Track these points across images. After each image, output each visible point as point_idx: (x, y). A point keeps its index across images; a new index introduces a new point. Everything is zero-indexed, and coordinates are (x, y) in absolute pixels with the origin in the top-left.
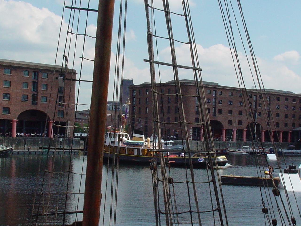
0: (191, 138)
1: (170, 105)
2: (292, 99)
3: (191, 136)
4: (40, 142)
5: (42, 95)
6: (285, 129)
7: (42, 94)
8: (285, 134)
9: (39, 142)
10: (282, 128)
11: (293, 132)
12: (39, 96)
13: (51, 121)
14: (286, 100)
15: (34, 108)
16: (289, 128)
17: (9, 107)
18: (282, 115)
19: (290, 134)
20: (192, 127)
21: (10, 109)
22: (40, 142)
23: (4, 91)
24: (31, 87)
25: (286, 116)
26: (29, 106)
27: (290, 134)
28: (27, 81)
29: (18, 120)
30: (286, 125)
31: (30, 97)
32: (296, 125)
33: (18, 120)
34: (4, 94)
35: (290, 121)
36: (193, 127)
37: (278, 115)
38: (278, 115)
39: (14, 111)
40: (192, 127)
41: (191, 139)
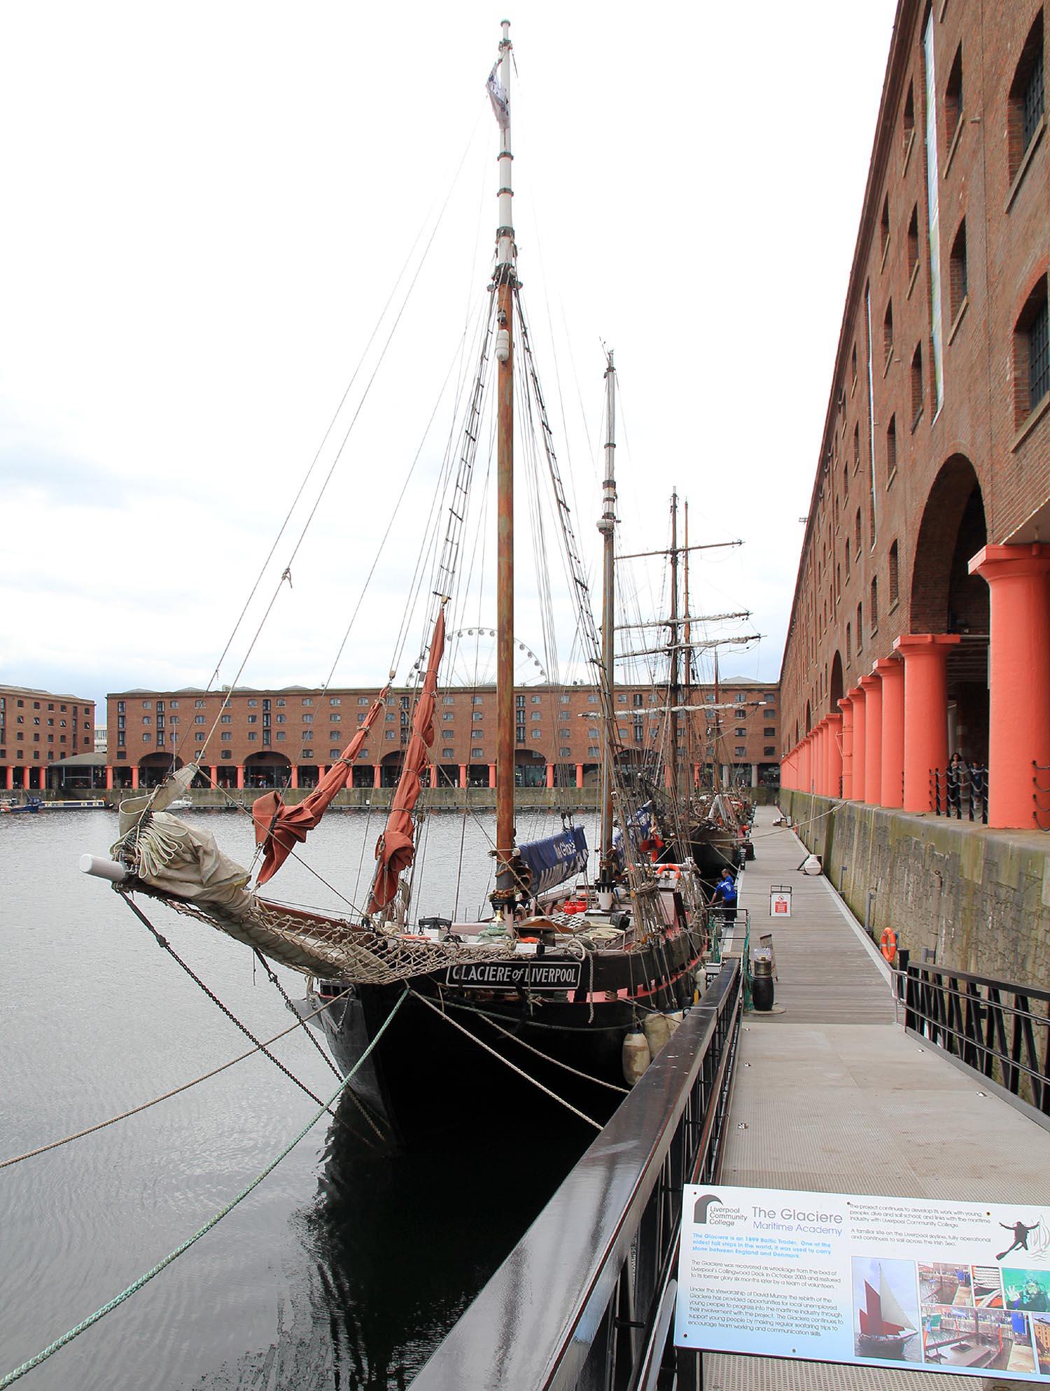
2: (47, 704)
6: (36, 764)
8: (35, 772)
10: (28, 762)
11: (50, 770)
14: (37, 706)
16: (44, 762)
18: (29, 737)
19: (43, 774)
25: (37, 737)
27: (43, 774)
30: (37, 755)
32: (57, 755)
35: (44, 747)
37: (20, 736)
38: (20, 736)
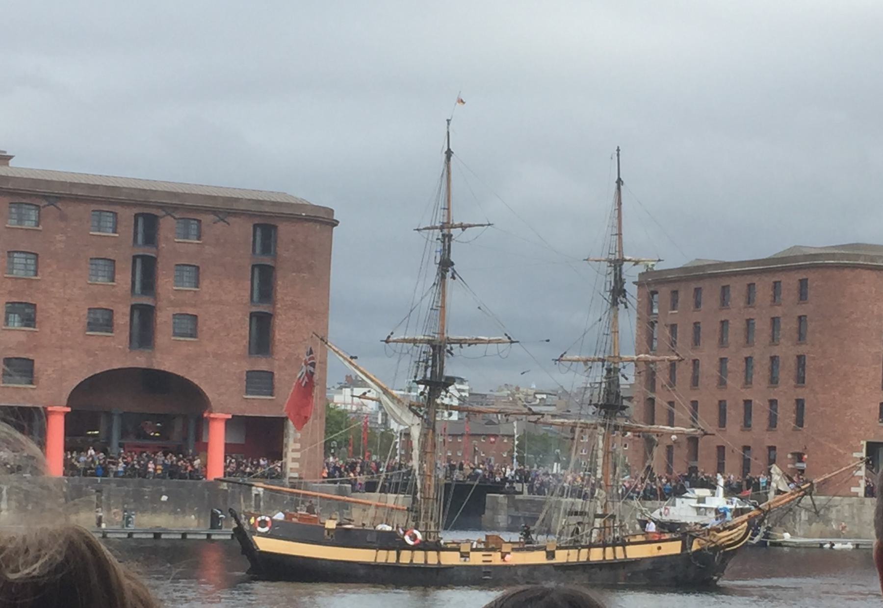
0: (859, 486)
1: (775, 351)
3: (861, 477)
4: (164, 498)
5: (177, 311)
7: (173, 304)
9: (161, 496)
12: (164, 317)
13: (212, 416)
15: (139, 360)
17: (30, 356)
20: (864, 443)
21: (37, 365)
22: (164, 498)
23: (10, 292)
24: (124, 279)
26: (115, 353)
28: (110, 253)
29: (69, 410)
31: (122, 319)
33: (69, 410)
34: (7, 303)
36: (868, 443)
39: (50, 371)
40: (863, 440)
41: (861, 490)
